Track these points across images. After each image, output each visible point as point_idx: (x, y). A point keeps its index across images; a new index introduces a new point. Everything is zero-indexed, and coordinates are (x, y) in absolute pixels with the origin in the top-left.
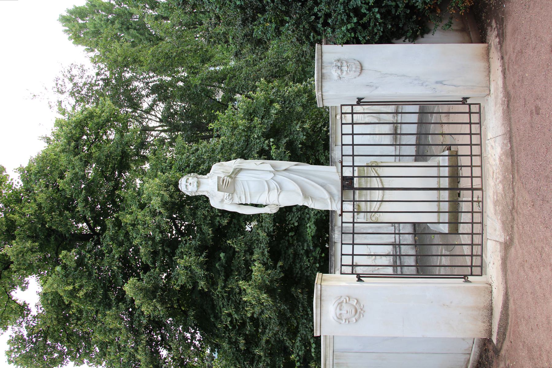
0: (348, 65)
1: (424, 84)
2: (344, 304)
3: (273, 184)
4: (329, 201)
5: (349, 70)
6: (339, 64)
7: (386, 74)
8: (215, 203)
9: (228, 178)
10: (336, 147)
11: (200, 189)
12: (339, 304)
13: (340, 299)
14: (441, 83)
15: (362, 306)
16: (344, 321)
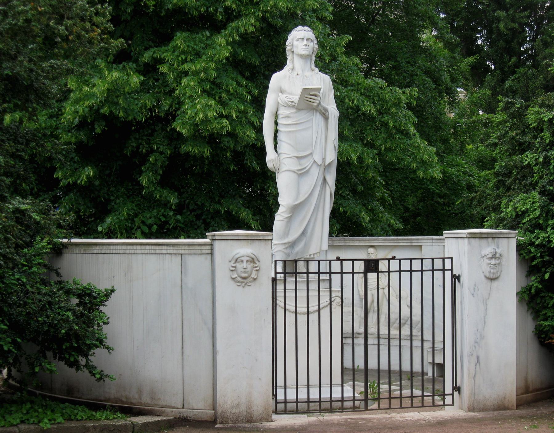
0: (497, 265)
1: (476, 344)
2: (252, 264)
3: (307, 163)
4: (286, 241)
5: (492, 266)
6: (497, 256)
7: (487, 305)
8: (276, 79)
9: (318, 102)
11: (296, 58)
12: (253, 259)
13: (257, 259)
14: (478, 361)
15: (250, 284)
16: (234, 265)
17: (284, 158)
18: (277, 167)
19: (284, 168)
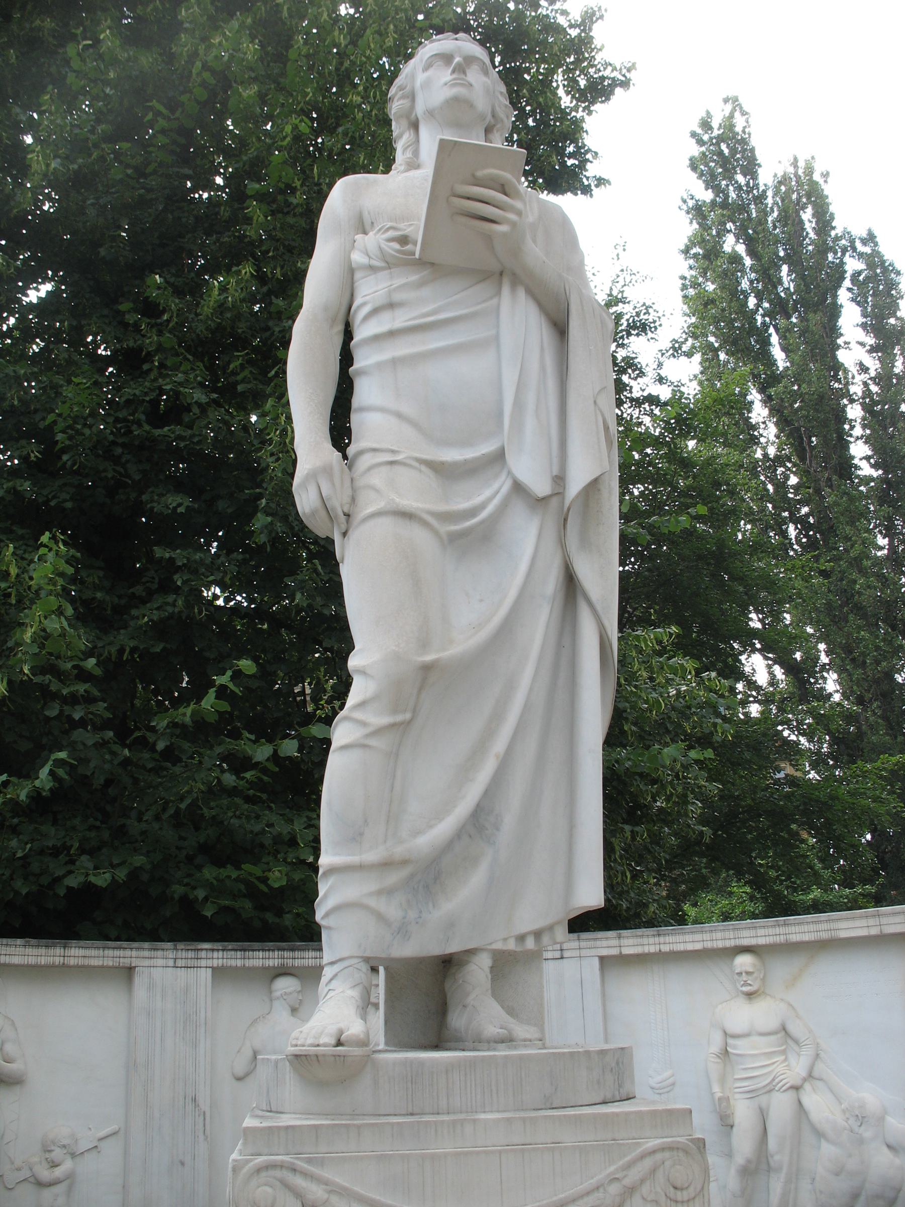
10: (596, 961)
17: (370, 469)
18: (338, 504)
19: (369, 505)
